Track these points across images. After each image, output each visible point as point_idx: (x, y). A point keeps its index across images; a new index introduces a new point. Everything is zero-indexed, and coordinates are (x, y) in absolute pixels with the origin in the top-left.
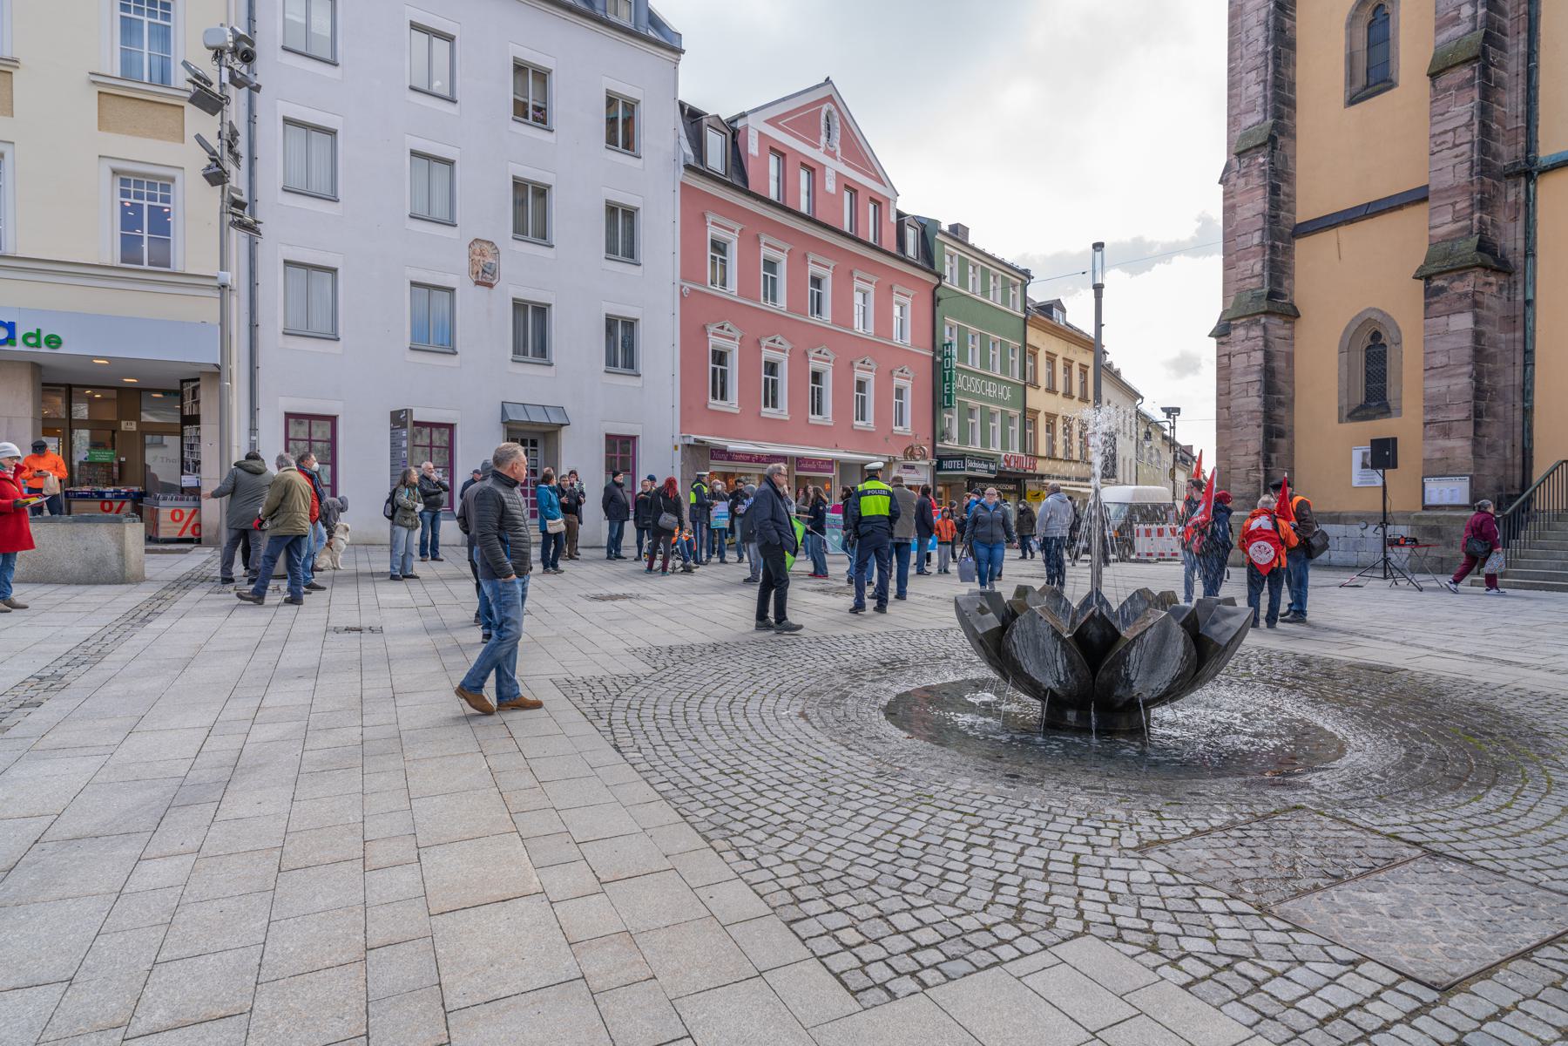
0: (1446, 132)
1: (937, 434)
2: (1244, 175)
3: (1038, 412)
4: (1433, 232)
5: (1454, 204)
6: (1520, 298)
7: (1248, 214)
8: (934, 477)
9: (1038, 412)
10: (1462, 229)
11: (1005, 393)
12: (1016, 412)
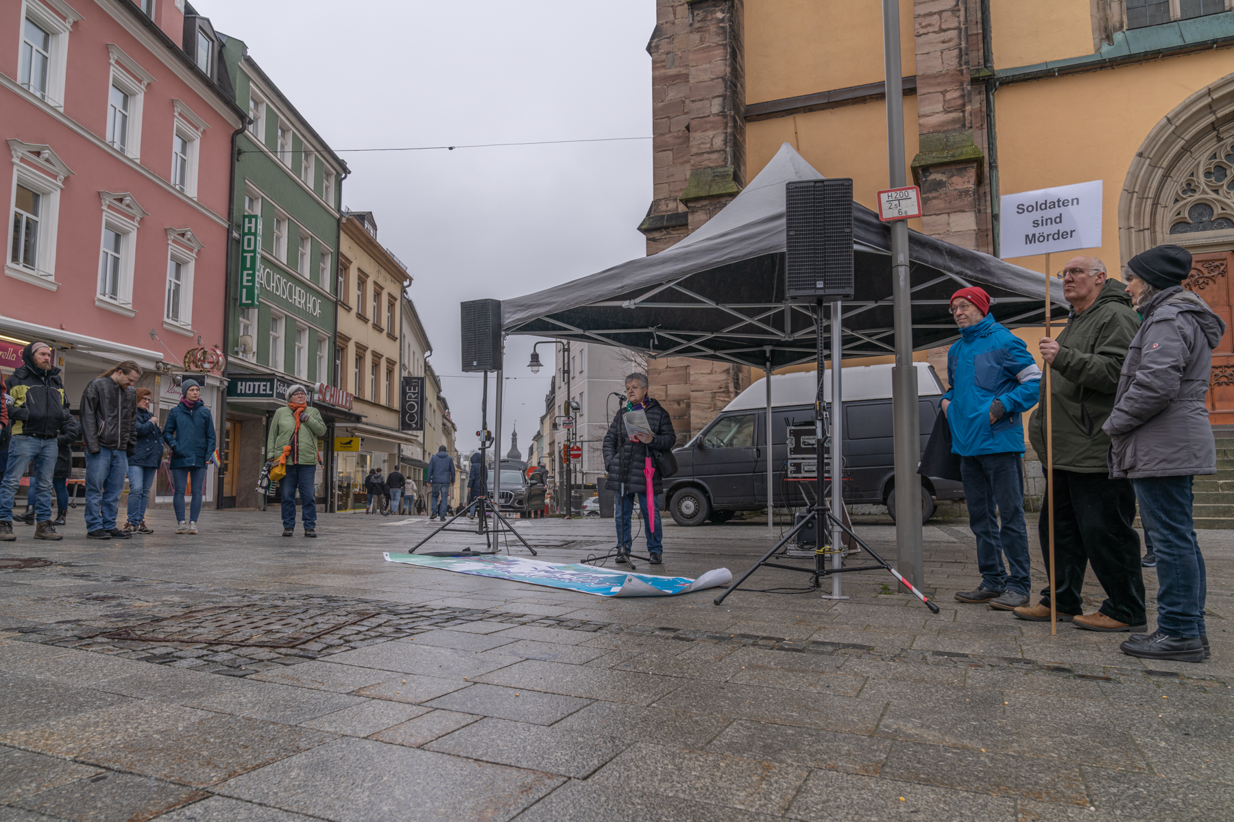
0: (931, 14)
1: (228, 343)
2: (699, 30)
3: (347, 339)
4: (922, 121)
5: (944, 93)
6: (989, 211)
7: (706, 77)
8: (223, 405)
9: (347, 339)
10: (954, 121)
11: (314, 307)
12: (326, 334)
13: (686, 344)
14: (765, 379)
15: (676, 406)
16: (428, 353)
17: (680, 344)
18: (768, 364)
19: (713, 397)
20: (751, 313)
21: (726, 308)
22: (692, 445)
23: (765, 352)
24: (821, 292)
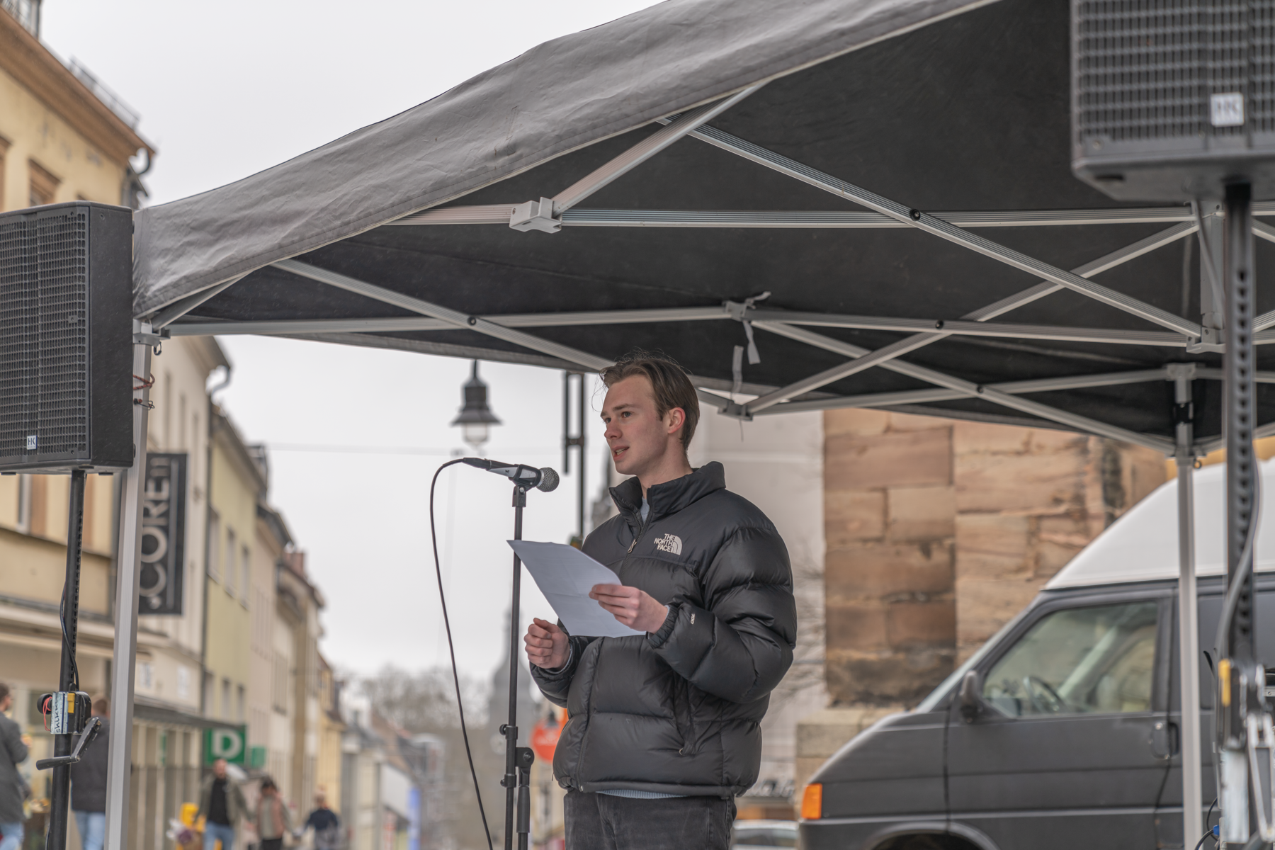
13: (861, 361)
14: (1173, 485)
15: (915, 559)
16: (217, 377)
17: (839, 360)
18: (1183, 430)
19: (1033, 534)
20: (1067, 250)
21: (954, 230)
22: (945, 705)
23: (1170, 386)
24: (1235, 147)
